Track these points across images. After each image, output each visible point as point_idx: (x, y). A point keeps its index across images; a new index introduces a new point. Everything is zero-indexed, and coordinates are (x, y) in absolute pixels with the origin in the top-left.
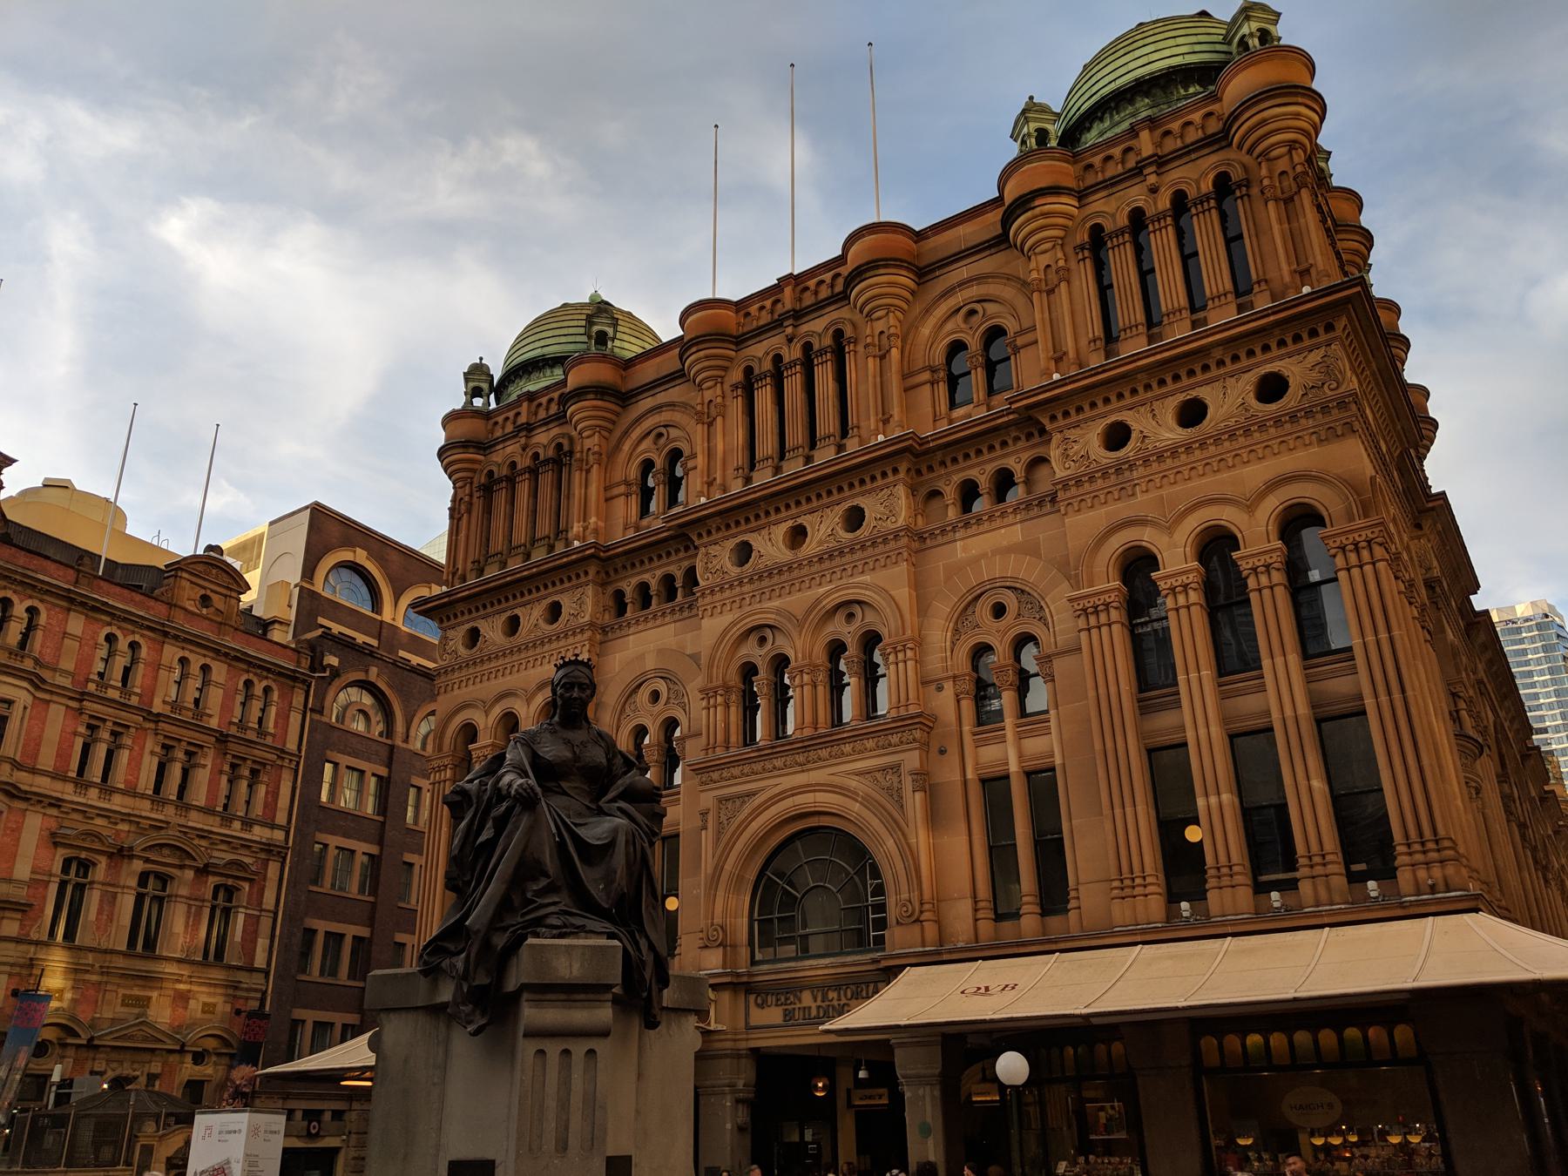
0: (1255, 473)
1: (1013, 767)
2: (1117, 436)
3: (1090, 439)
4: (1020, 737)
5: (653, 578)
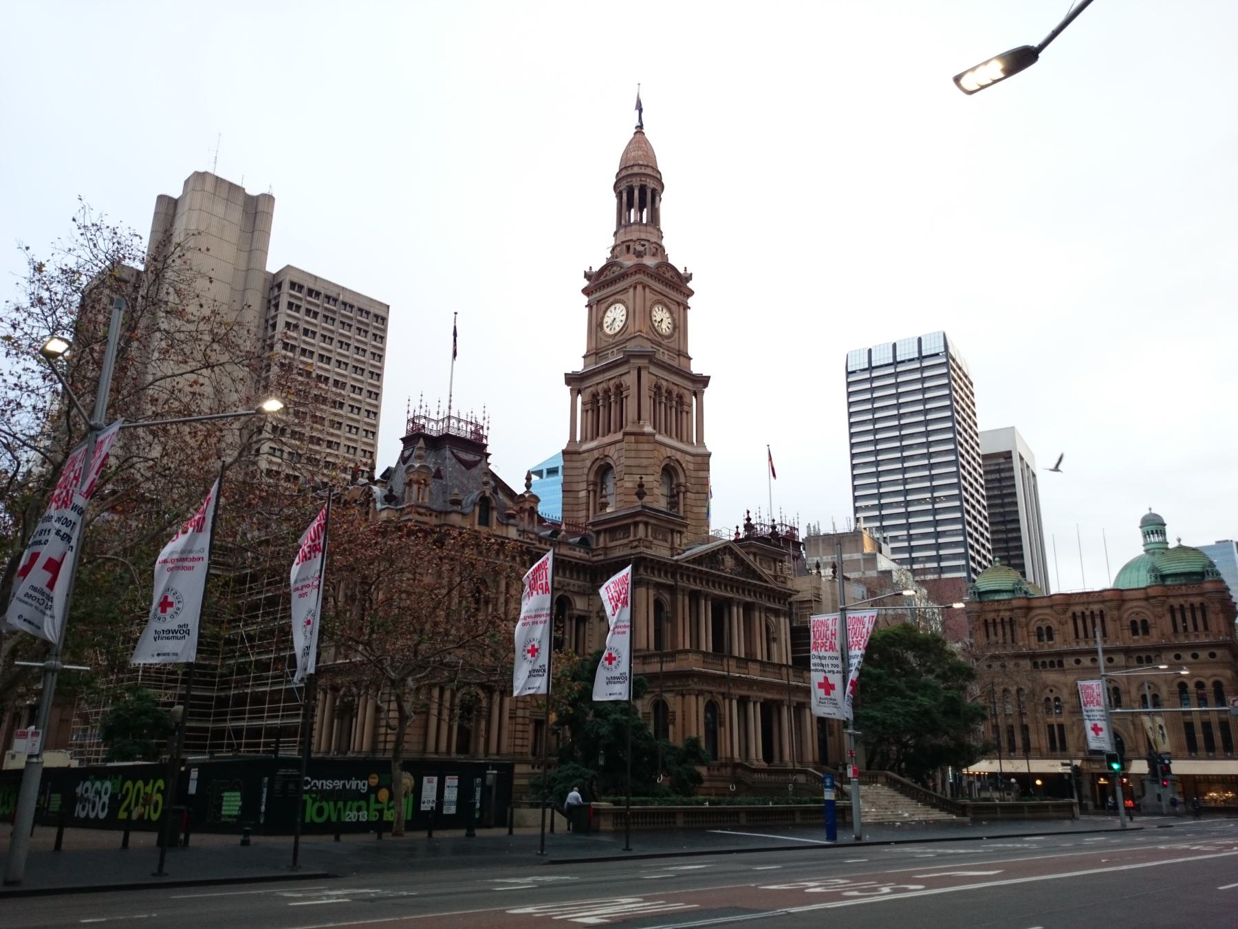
5: (1048, 660)
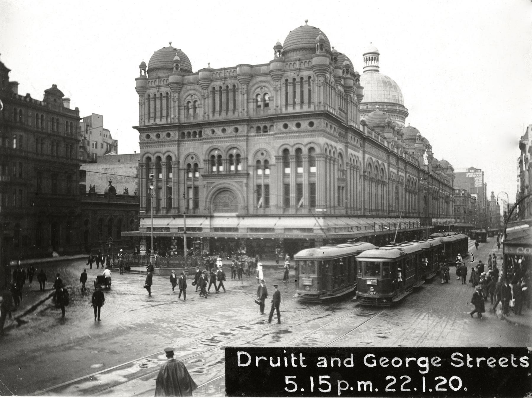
0: (306, 140)
1: (263, 184)
2: (286, 126)
3: (280, 125)
4: (264, 178)
5: (192, 131)
